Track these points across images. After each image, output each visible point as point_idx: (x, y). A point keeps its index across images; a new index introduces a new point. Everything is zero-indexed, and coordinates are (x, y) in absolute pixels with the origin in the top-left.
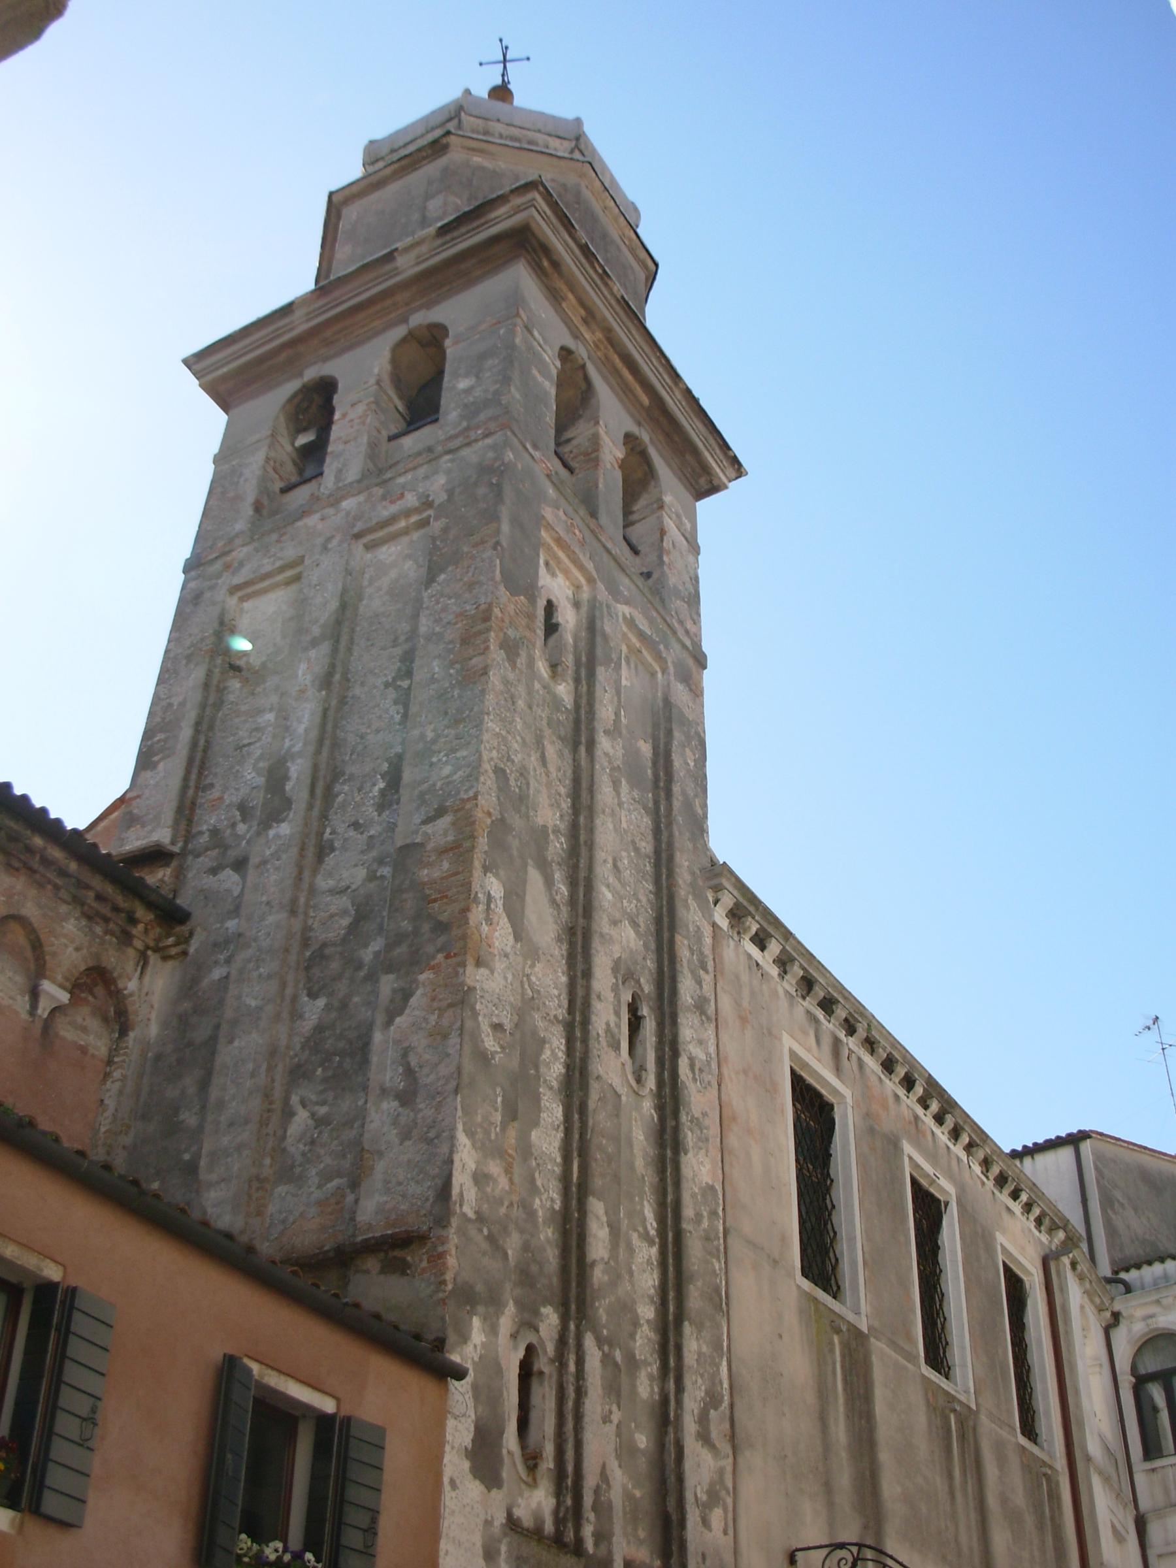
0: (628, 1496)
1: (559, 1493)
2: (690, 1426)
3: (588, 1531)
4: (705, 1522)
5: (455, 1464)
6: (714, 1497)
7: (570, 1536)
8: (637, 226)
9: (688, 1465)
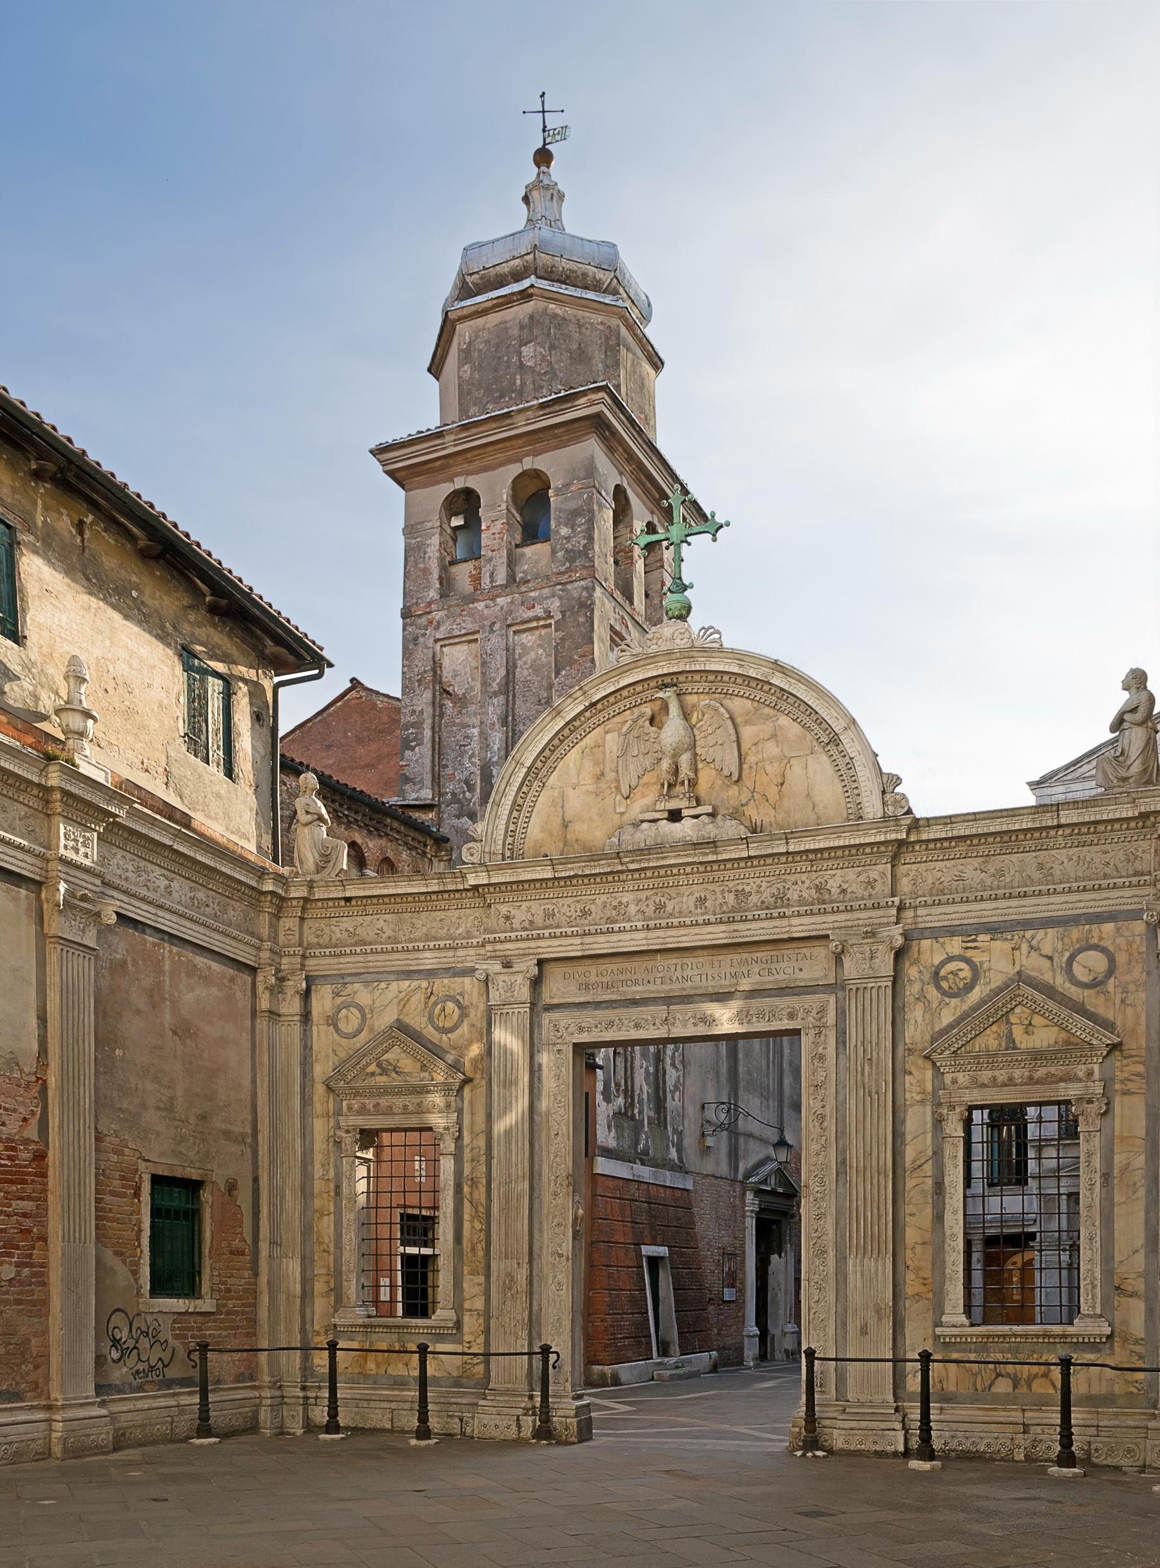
0: (648, 1092)
1: (625, 1098)
2: (668, 1061)
3: (636, 1111)
4: (673, 1099)
5: (599, 1098)
6: (676, 1088)
7: (629, 1114)
8: (646, 319)
9: (667, 1077)
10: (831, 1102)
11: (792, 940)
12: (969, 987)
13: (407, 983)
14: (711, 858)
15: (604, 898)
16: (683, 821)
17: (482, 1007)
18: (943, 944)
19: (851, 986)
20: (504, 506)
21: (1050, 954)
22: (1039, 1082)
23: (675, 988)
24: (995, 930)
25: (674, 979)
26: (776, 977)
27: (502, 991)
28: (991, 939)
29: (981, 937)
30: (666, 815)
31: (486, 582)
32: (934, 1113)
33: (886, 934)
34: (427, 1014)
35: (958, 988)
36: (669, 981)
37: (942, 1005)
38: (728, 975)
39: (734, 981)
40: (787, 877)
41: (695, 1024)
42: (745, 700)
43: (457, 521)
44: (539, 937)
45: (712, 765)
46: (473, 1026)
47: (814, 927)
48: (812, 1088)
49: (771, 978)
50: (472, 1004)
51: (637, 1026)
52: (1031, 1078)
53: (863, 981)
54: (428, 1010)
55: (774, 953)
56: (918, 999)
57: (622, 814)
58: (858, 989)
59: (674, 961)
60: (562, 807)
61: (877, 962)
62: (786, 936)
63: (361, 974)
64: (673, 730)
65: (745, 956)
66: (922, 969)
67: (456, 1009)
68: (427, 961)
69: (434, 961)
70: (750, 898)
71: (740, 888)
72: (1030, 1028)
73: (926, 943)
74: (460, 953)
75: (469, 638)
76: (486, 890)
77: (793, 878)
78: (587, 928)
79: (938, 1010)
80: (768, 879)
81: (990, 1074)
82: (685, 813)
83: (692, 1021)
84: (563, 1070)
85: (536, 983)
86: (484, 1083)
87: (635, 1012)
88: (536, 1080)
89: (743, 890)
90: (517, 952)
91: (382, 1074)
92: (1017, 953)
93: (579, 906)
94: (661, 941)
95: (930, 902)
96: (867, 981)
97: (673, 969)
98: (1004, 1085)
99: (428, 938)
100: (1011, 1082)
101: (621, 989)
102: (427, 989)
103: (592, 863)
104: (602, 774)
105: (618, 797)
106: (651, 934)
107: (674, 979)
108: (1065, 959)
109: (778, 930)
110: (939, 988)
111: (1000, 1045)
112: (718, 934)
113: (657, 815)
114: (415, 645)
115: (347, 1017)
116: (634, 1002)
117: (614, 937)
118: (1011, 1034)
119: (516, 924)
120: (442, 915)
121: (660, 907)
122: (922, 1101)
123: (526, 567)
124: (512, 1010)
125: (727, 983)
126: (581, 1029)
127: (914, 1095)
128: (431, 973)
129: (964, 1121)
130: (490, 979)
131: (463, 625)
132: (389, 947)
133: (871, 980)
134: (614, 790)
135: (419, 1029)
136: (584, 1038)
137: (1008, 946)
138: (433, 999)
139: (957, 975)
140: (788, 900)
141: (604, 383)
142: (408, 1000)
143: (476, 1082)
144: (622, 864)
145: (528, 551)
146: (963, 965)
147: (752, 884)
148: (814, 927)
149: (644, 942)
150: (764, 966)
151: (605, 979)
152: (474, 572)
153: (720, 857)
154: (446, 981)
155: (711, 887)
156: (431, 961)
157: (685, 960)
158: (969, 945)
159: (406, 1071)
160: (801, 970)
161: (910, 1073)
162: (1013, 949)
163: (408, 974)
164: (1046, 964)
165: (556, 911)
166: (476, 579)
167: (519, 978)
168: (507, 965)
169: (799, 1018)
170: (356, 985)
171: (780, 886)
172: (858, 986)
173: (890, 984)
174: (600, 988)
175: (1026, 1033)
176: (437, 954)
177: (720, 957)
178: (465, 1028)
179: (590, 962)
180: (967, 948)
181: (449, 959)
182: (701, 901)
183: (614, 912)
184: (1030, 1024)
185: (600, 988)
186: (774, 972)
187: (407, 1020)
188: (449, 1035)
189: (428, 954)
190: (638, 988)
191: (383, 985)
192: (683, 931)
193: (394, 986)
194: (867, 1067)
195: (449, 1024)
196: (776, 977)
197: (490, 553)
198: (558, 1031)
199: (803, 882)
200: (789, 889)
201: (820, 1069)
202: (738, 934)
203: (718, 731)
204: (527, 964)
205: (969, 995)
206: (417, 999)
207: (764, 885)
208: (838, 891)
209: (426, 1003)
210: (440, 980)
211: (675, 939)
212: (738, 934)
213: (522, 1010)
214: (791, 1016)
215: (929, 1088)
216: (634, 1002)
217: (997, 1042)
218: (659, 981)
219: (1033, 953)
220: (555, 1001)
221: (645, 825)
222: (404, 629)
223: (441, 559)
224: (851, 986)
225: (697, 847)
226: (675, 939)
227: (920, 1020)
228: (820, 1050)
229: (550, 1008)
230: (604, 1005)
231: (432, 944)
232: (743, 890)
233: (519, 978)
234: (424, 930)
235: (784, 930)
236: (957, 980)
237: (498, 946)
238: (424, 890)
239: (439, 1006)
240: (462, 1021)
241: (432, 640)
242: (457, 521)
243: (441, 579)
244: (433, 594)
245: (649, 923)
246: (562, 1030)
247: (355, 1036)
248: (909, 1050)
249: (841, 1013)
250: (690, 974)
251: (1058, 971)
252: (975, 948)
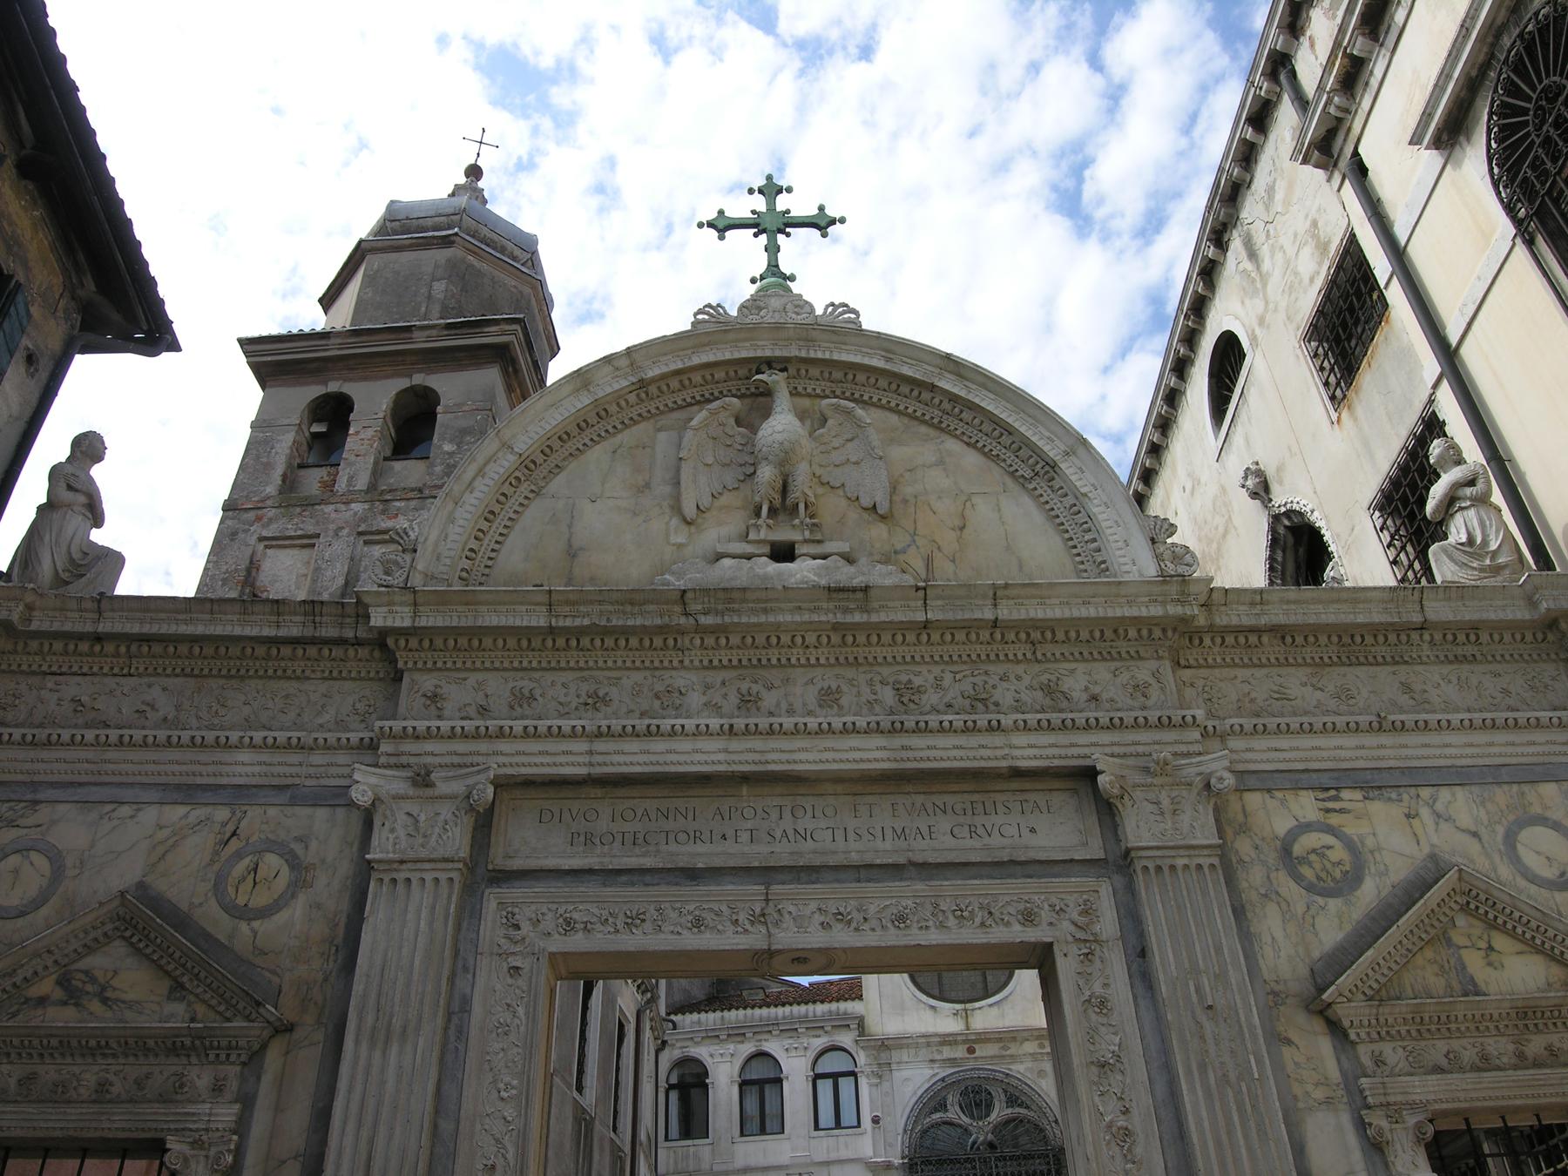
10: (1142, 1102)
11: (1017, 773)
12: (1352, 879)
13: (181, 810)
14: (858, 618)
15: (637, 677)
16: (798, 561)
17: (345, 868)
18: (1283, 802)
19: (1144, 862)
20: (381, 415)
21: (1473, 829)
22: (1537, 1064)
23: (782, 853)
24: (1374, 783)
25: (778, 834)
26: (987, 840)
27: (401, 833)
28: (1365, 798)
29: (1345, 794)
30: (767, 550)
31: (341, 485)
32: (1361, 1125)
33: (1193, 770)
34: (212, 876)
35: (1334, 879)
36: (769, 839)
37: (1313, 911)
38: (888, 832)
39: (902, 844)
40: (991, 668)
41: (825, 926)
42: (888, 414)
43: (317, 428)
44: (501, 734)
45: (841, 492)
46: (319, 906)
47: (1056, 751)
48: (1094, 1069)
49: (976, 843)
50: (323, 861)
51: (698, 924)
52: (1521, 1056)
53: (1167, 853)
54: (216, 867)
55: (976, 797)
56: (1266, 896)
57: (680, 546)
58: (1159, 868)
59: (777, 801)
60: (570, 526)
61: (1185, 819)
62: (1004, 764)
63: (81, 784)
64: (781, 425)
65: (919, 799)
66: (1258, 842)
67: (285, 870)
68: (239, 769)
69: (257, 769)
70: (925, 697)
71: (904, 678)
72: (1494, 957)
73: (1254, 800)
74: (317, 758)
75: (307, 541)
76: (402, 643)
77: (1000, 669)
78: (604, 723)
79: (1308, 918)
80: (955, 668)
81: (1442, 1046)
82: (799, 550)
83: (818, 918)
84: (521, 1011)
85: (484, 824)
86: (319, 1036)
87: (693, 897)
88: (452, 1032)
89: (910, 681)
90: (447, 760)
91: (65, 1003)
92: (1415, 822)
93: (585, 688)
94: (757, 757)
95: (1248, 727)
96: (1172, 853)
97: (774, 815)
98: (1476, 1069)
99: (248, 724)
100: (1485, 1063)
101: (663, 847)
102: (224, 824)
103: (628, 608)
104: (647, 485)
105: (675, 521)
106: (735, 745)
107: (778, 834)
108: (1500, 838)
109: (988, 753)
110: (1298, 878)
111: (1449, 986)
112: (873, 754)
113: (749, 549)
114: (232, 540)
115: (16, 872)
116: (692, 875)
117: (659, 745)
118: (1464, 967)
119: (449, 707)
120: (291, 687)
121: (748, 702)
122: (1328, 1102)
123: (392, 481)
124: (418, 875)
125: (888, 845)
126: (569, 926)
127: (1310, 1088)
128: (241, 794)
129: (1428, 1147)
130: (381, 809)
131: (301, 526)
132: (162, 735)
133: (1182, 852)
134: (667, 510)
135: (184, 906)
136: (578, 942)
137: (1397, 811)
138: (234, 844)
139: (1323, 855)
140: (997, 704)
141: (521, 316)
142: (174, 846)
143: (298, 1034)
144: (687, 614)
145: (398, 466)
146: (1329, 839)
147: (925, 672)
148: (1056, 751)
149: (721, 757)
150: (961, 819)
151: (629, 827)
152: (326, 478)
153: (874, 618)
154: (272, 811)
155: (850, 673)
156: (249, 769)
157: (800, 800)
158: (1330, 805)
159: (130, 996)
160: (1033, 830)
161: (1289, 1042)
162: (1408, 816)
163: (188, 792)
164: (1474, 847)
165: (537, 693)
166: (329, 486)
167: (446, 810)
168: (422, 780)
169: (1044, 924)
170: (62, 808)
171: (979, 680)
172: (1159, 862)
173: (1216, 861)
174: (618, 843)
175: (1490, 964)
176: (265, 757)
177: (870, 799)
178: (296, 912)
179: (599, 792)
180: (1328, 811)
181: (287, 766)
182: (829, 698)
183: (657, 703)
184: (1491, 948)
185: (618, 843)
186: (980, 831)
187: (161, 885)
188: (256, 924)
189: (245, 756)
190: (700, 848)
191: (125, 810)
192: (799, 743)
193: (150, 815)
194: (1208, 1027)
195: (261, 899)
196: (987, 840)
197: (353, 458)
198: (517, 927)
199: (1019, 678)
200: (994, 687)
201: (1103, 1029)
202: (910, 754)
203: (849, 445)
204: (470, 781)
205: (1358, 893)
206: (196, 849)
207: (948, 678)
208: (1085, 696)
209: (216, 853)
210: (258, 810)
211: (785, 757)
212: (910, 754)
213: (443, 876)
214: (1028, 918)
215: (1334, 1074)
216: (692, 875)
217: (1443, 981)
218: (745, 837)
219: (1444, 826)
220: (517, 864)
221: (727, 562)
222: (222, 522)
223: (290, 457)
224: (1144, 862)
225: (834, 595)
226: (785, 757)
227: (1279, 934)
228: (1098, 988)
229: (503, 877)
230: (624, 878)
231: (258, 736)
232: (910, 681)
233: (446, 810)
234: (246, 710)
235: (999, 753)
236: (1329, 866)
237: (409, 746)
238: (268, 632)
239: (246, 861)
240: (293, 896)
241: (255, 537)
242: (317, 428)
243: (284, 477)
244: (271, 490)
245: (734, 721)
246: (526, 927)
247: (22, 914)
248: (1275, 994)
249: (1131, 917)
250: (810, 827)
251: (1497, 858)
252: (1341, 811)
